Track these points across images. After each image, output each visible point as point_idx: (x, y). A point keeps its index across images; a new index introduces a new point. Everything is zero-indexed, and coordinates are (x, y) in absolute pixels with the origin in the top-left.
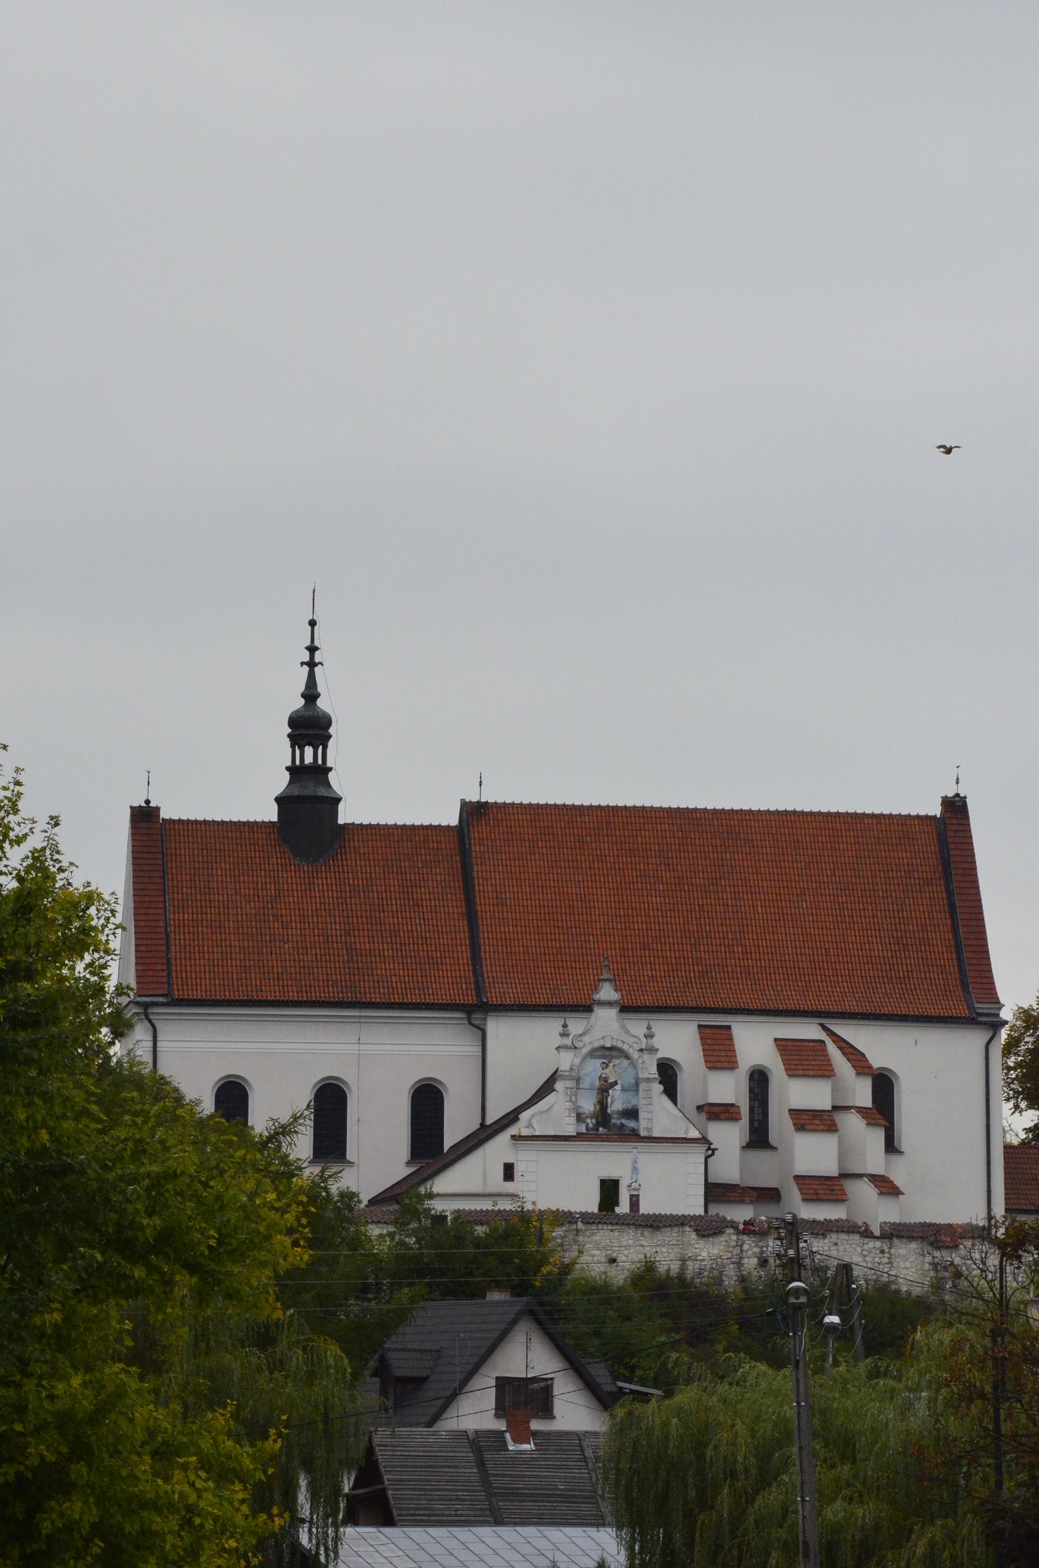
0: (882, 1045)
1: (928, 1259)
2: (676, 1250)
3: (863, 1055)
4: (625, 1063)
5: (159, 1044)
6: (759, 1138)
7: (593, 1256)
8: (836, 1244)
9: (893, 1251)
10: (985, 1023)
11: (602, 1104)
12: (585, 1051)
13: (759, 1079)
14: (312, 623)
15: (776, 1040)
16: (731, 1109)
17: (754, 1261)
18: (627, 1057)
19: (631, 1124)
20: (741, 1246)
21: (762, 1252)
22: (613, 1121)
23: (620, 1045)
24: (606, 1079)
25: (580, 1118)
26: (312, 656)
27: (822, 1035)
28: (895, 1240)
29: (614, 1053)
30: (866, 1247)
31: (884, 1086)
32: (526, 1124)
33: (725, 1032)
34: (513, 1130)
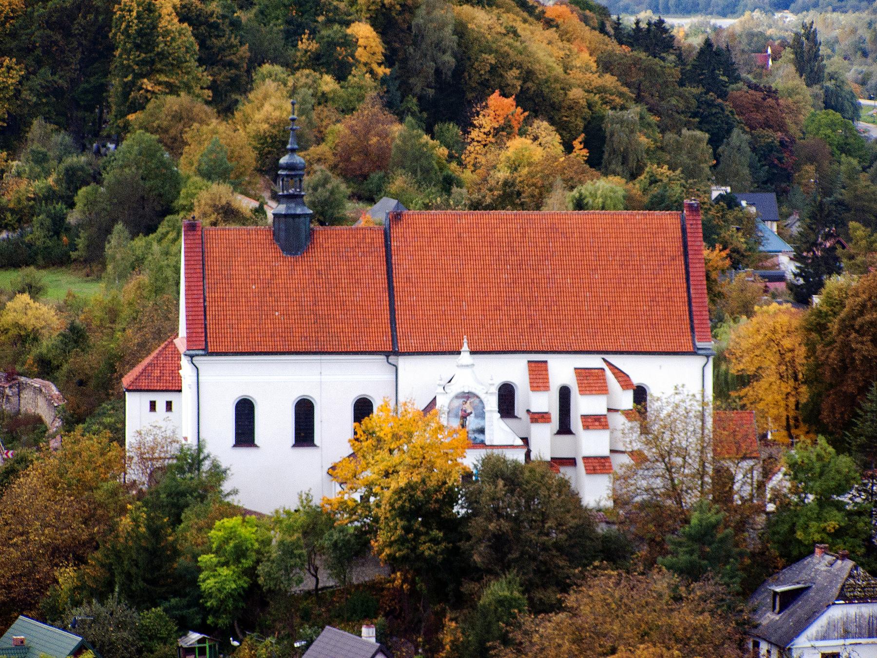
3: (628, 376)
4: (477, 401)
5: (200, 378)
6: (565, 429)
12: (453, 394)
13: (565, 394)
18: (478, 397)
19: (480, 437)
24: (465, 411)
27: (604, 366)
31: (640, 394)
33: (543, 365)
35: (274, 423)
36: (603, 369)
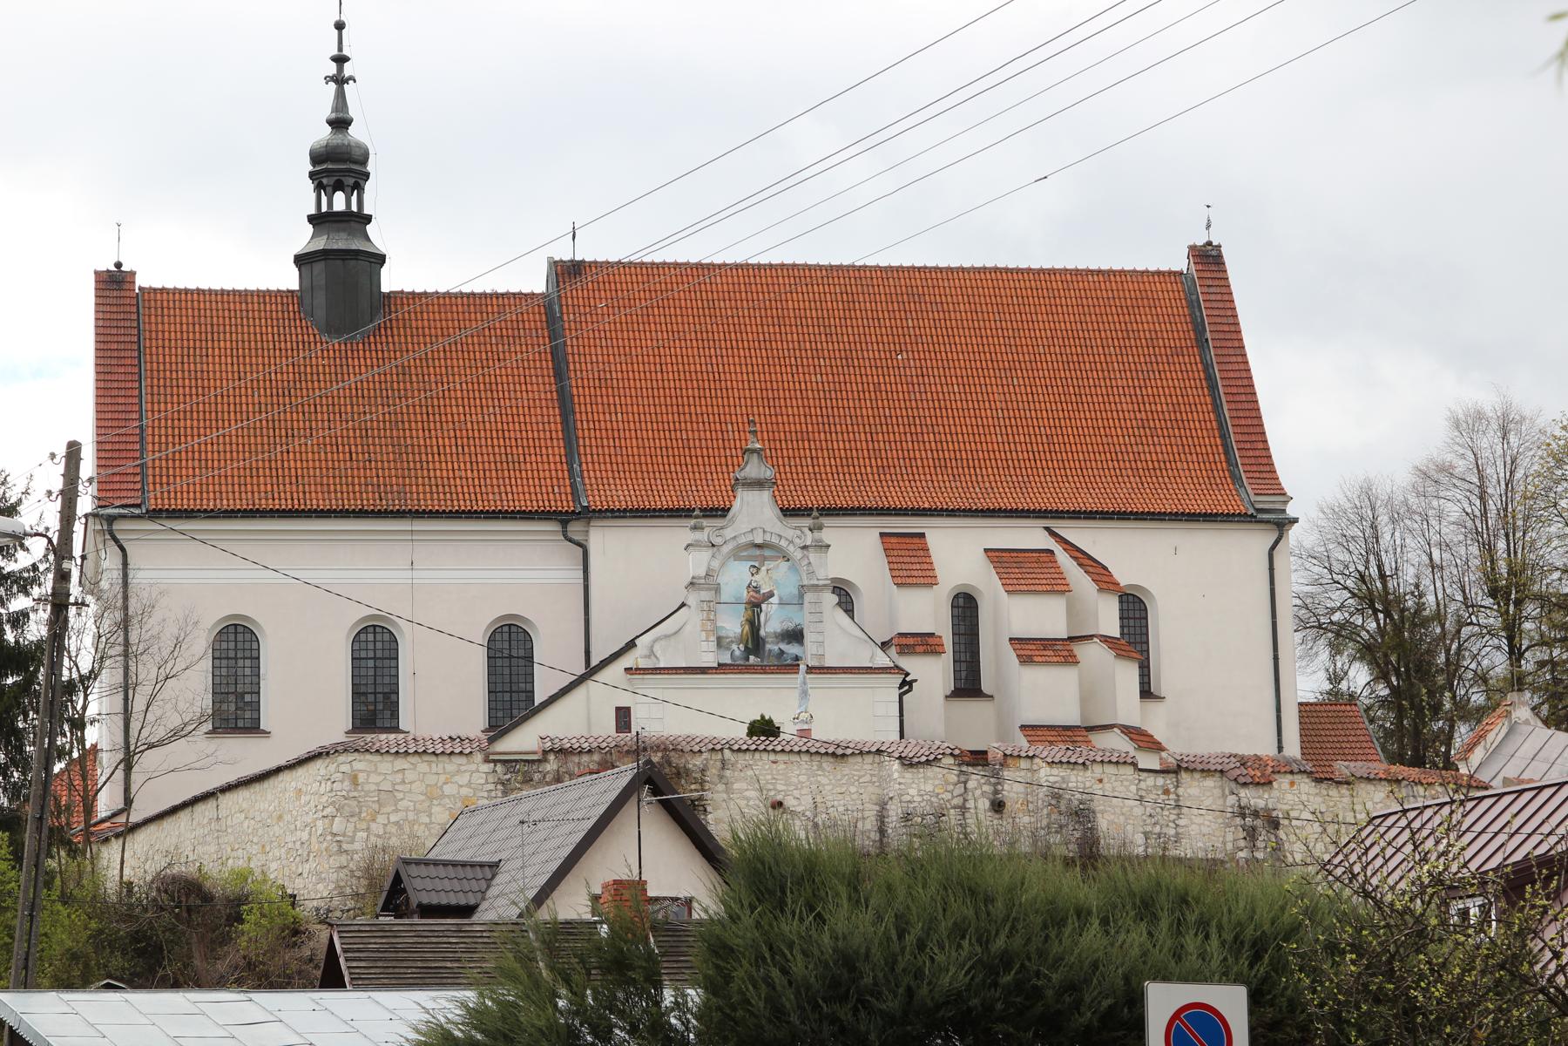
0: (1130, 553)
1: (1232, 800)
2: (871, 789)
3: (1105, 568)
4: (784, 565)
5: (131, 574)
6: (968, 686)
7: (748, 799)
8: (1101, 781)
9: (1181, 791)
10: (1268, 522)
11: (754, 625)
12: (726, 549)
13: (965, 607)
14: (340, 26)
15: (986, 550)
16: (931, 641)
17: (984, 804)
19: (792, 649)
20: (965, 783)
21: (996, 792)
22: (768, 646)
23: (775, 540)
24: (756, 589)
25: (720, 643)
26: (340, 69)
27: (1050, 543)
28: (1184, 775)
29: (767, 553)
30: (1143, 785)
31: (1134, 608)
32: (646, 652)
33: (916, 540)
34: (628, 661)
35: (306, 692)
36: (1052, 552)
